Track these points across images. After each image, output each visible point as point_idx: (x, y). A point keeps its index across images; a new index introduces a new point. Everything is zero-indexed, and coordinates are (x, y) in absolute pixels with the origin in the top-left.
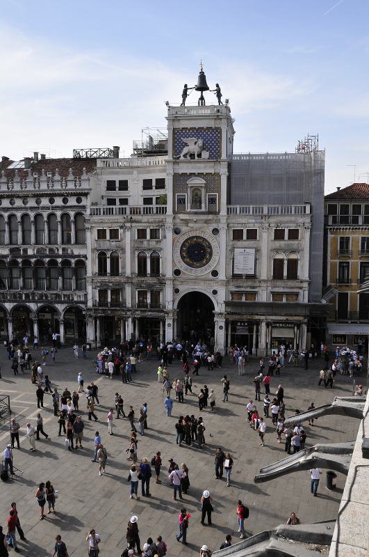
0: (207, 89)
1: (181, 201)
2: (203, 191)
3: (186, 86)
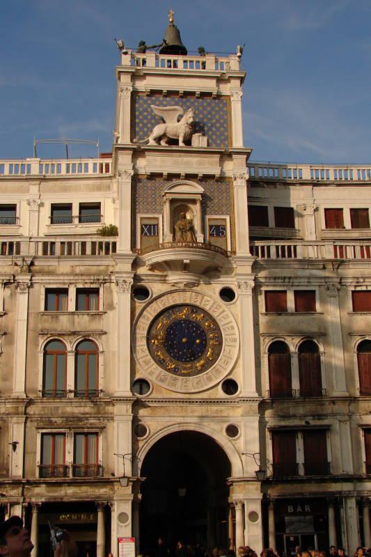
1: (151, 230)
2: (196, 208)
3: (143, 43)
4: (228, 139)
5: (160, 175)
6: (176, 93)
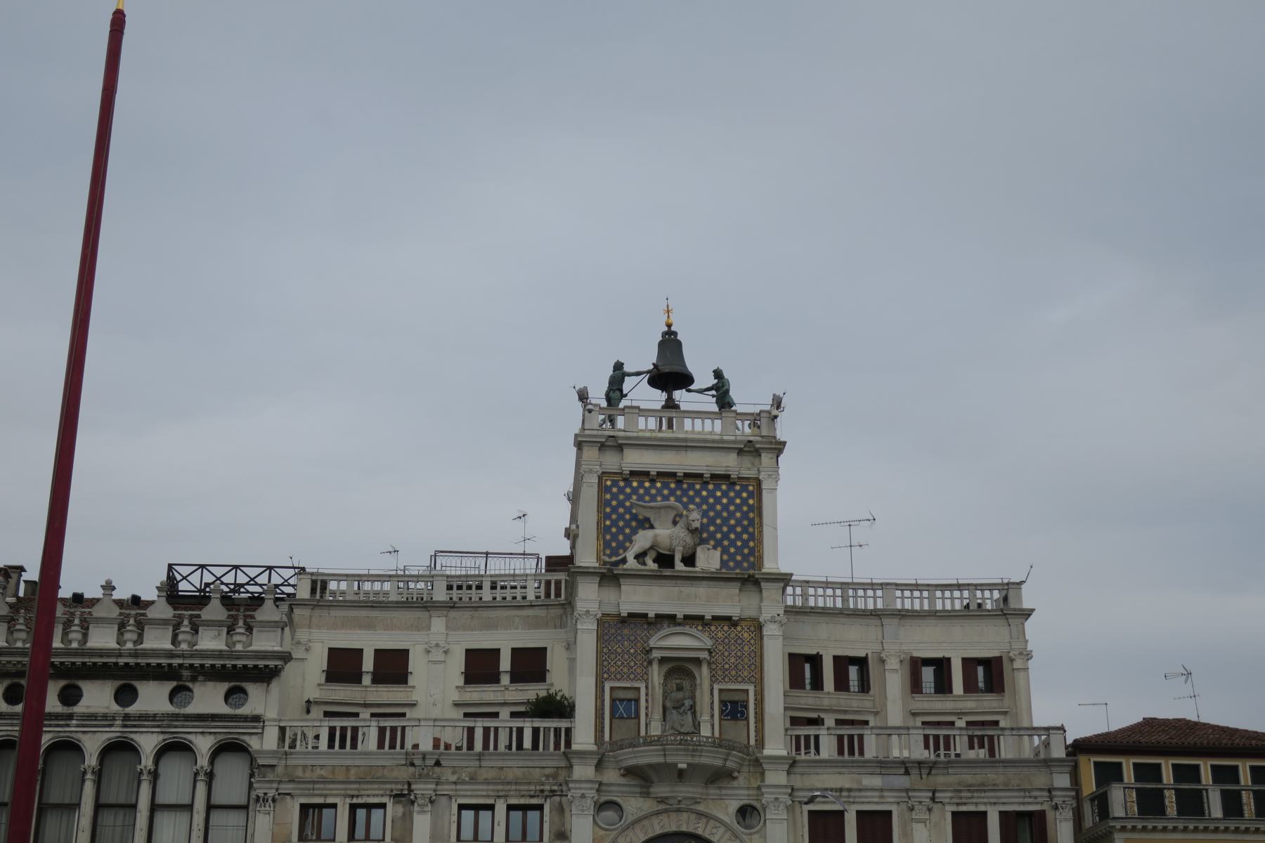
0: (683, 380)
3: (618, 366)
4: (754, 553)
5: (645, 616)
6: (673, 475)
